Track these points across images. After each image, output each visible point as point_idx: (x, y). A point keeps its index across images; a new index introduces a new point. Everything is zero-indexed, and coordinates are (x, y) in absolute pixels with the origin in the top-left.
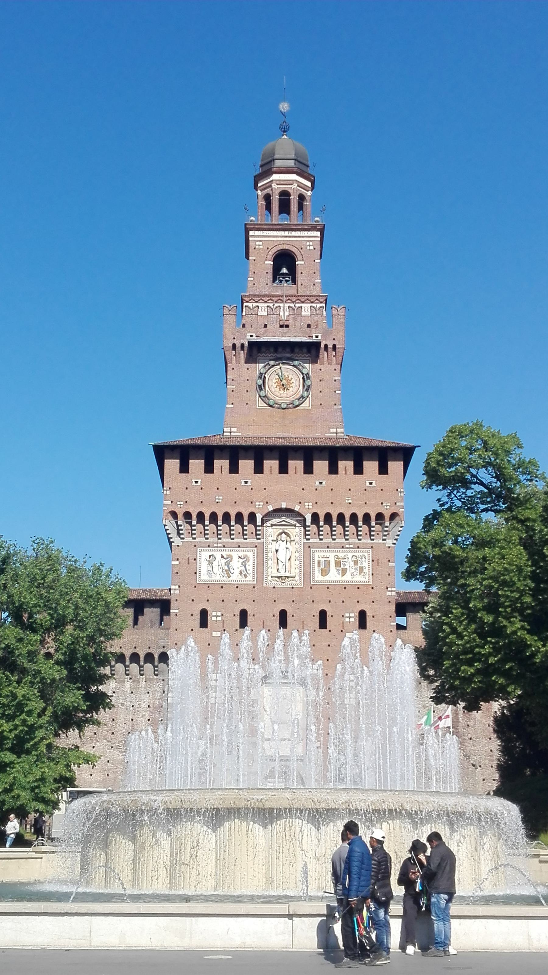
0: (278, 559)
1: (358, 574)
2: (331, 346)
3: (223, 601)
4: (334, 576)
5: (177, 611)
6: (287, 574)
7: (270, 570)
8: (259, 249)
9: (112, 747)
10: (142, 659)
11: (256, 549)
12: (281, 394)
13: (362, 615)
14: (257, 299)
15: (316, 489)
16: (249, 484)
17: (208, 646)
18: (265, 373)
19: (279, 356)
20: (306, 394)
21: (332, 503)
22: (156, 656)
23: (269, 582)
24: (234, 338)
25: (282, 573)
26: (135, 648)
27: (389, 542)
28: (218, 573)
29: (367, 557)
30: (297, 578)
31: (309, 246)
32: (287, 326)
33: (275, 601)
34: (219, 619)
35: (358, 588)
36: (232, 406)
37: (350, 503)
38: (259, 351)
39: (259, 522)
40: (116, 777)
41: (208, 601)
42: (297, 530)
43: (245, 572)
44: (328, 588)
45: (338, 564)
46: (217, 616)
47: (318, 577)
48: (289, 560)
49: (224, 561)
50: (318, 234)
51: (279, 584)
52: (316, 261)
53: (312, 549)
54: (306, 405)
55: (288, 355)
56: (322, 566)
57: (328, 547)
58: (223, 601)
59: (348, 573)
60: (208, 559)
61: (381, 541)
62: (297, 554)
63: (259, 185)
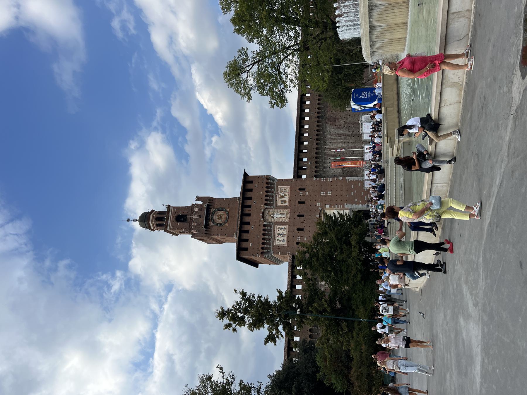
4: (287, 199)
6: (285, 214)
7: (283, 220)
13: (300, 189)
14: (190, 227)
16: (253, 227)
19: (210, 219)
20: (224, 210)
23: (287, 221)
25: (285, 216)
27: (276, 181)
39: (266, 223)
42: (270, 211)
45: (282, 197)
46: (299, 239)
47: (287, 204)
49: (280, 236)
54: (228, 209)
55: (211, 215)
56: (283, 202)
59: (286, 194)
61: (276, 183)
63: (152, 228)
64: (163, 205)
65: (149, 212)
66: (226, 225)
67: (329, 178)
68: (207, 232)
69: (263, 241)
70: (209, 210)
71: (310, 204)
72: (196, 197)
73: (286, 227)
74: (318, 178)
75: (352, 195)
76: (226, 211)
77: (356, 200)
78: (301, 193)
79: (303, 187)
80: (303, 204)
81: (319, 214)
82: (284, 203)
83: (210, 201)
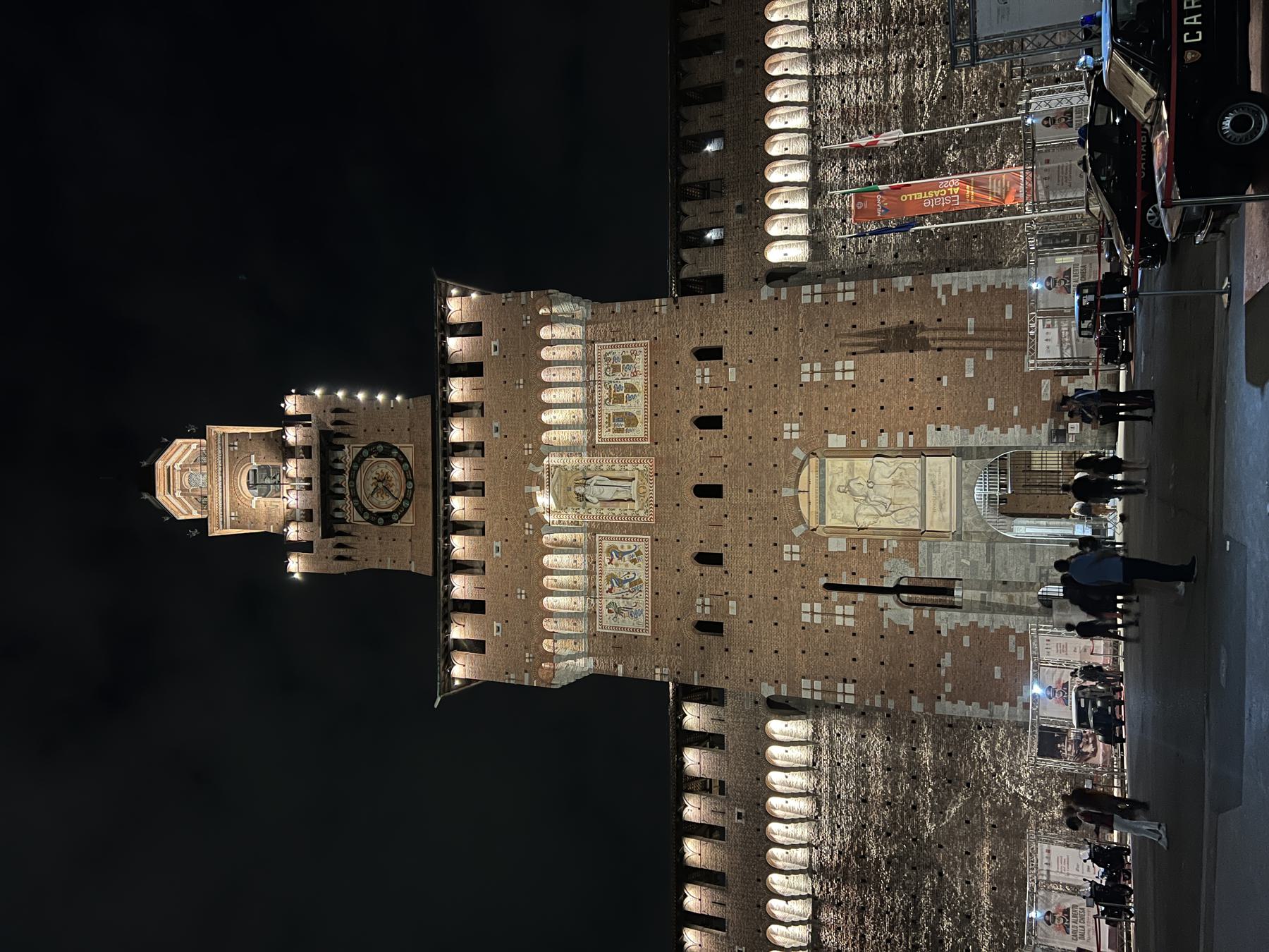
1: (633, 364)
2: (333, 415)
4: (638, 405)
5: (696, 673)
7: (629, 513)
9: (941, 813)
11: (598, 535)
12: (396, 490)
15: (506, 436)
16: (499, 544)
17: (753, 625)
18: (370, 512)
19: (348, 492)
21: (525, 411)
28: (636, 600)
29: (608, 351)
30: (641, 467)
32: (311, 479)
34: (707, 601)
35: (656, 363)
36: (413, 563)
37: (524, 381)
40: (999, 810)
43: (633, 553)
44: (656, 415)
45: (619, 399)
47: (640, 431)
48: (611, 479)
53: (597, 442)
54: (408, 452)
57: (594, 416)
60: (614, 614)
62: (605, 467)
66: (409, 518)
67: (840, 286)
68: (342, 552)
71: (749, 432)
73: (642, 544)
74: (784, 290)
75: (970, 374)
76: (402, 459)
77: (991, 402)
78: (704, 373)
81: (793, 479)
82: (628, 425)
83: (340, 417)
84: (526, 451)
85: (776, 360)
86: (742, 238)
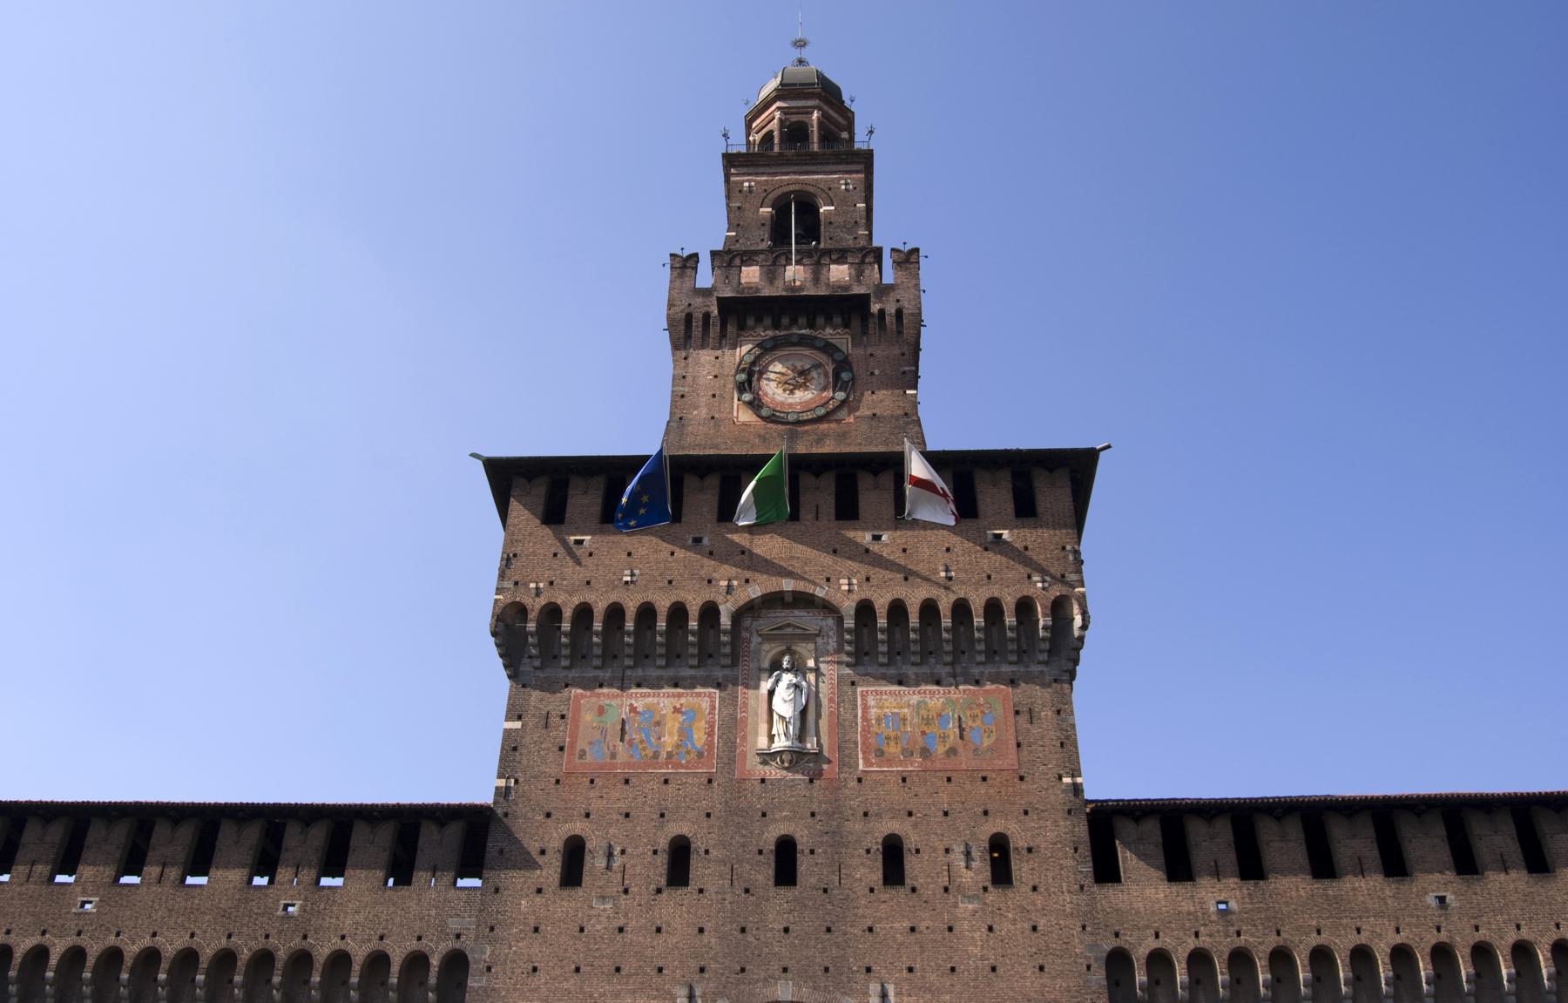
0: (770, 711)
2: (893, 311)
3: (627, 815)
8: (751, 192)
10: (395, 968)
11: (718, 692)
13: (999, 848)
16: (706, 541)
20: (841, 395)
22: (435, 962)
24: (690, 305)
26: (381, 938)
31: (846, 184)
33: (764, 815)
34: (617, 863)
38: (742, 327)
39: (725, 621)
41: (588, 815)
50: (861, 167)
51: (773, 772)
52: (858, 205)
53: (859, 689)
58: (627, 815)
63: (754, 125)
64: (871, 132)
65: (843, 102)
66: (745, 416)
69: (600, 608)
70: (838, 320)
72: (916, 250)
79: (1021, 869)
80: (878, 876)
84: (846, 581)
85: (994, 969)
86: (1180, 912)
